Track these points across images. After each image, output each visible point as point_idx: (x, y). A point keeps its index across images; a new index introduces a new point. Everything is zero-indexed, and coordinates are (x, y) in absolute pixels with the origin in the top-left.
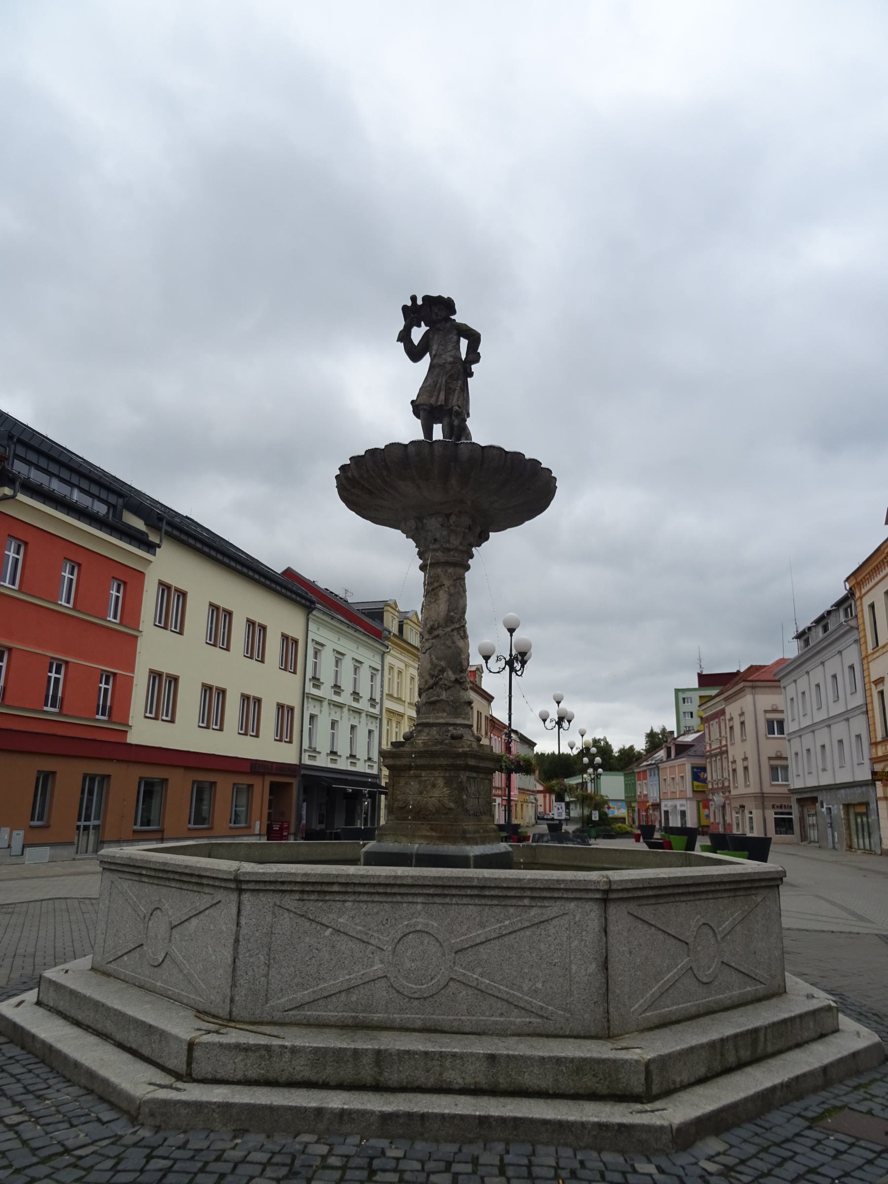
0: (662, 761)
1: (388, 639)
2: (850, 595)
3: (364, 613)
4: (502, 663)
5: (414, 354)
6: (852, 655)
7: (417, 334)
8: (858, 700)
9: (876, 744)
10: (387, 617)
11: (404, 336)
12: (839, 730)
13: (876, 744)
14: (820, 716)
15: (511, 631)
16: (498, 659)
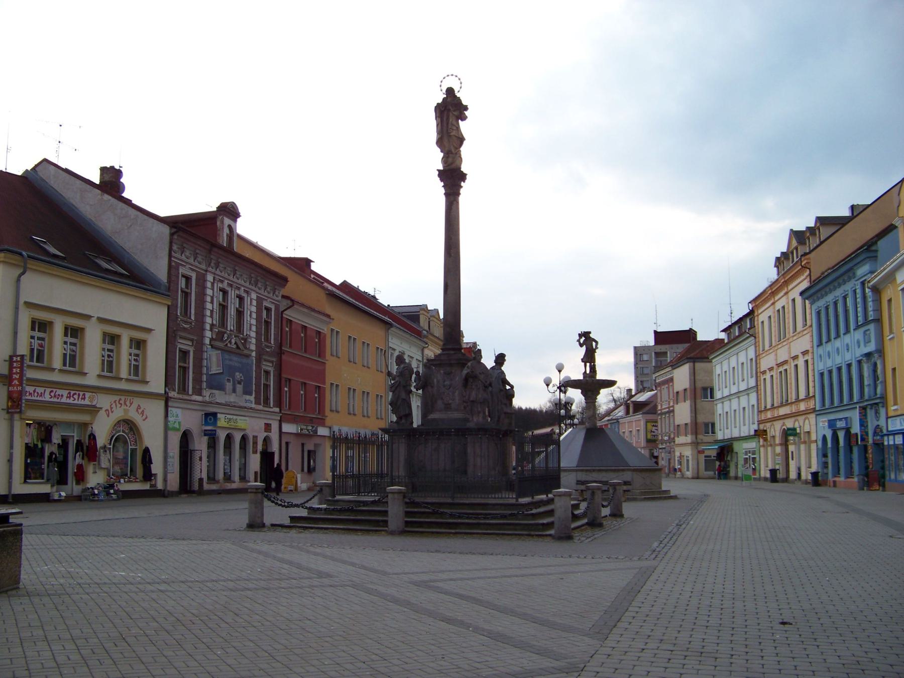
0: (622, 418)
1: (425, 337)
2: (751, 314)
3: (404, 316)
4: (556, 388)
5: (581, 345)
6: (751, 353)
7: (582, 340)
8: (752, 383)
9: (761, 412)
10: (422, 319)
11: (579, 341)
12: (744, 401)
13: (761, 412)
14: (734, 390)
15: (560, 371)
16: (554, 386)
